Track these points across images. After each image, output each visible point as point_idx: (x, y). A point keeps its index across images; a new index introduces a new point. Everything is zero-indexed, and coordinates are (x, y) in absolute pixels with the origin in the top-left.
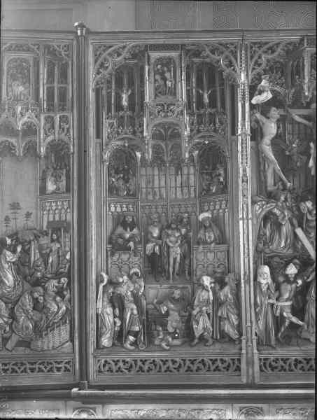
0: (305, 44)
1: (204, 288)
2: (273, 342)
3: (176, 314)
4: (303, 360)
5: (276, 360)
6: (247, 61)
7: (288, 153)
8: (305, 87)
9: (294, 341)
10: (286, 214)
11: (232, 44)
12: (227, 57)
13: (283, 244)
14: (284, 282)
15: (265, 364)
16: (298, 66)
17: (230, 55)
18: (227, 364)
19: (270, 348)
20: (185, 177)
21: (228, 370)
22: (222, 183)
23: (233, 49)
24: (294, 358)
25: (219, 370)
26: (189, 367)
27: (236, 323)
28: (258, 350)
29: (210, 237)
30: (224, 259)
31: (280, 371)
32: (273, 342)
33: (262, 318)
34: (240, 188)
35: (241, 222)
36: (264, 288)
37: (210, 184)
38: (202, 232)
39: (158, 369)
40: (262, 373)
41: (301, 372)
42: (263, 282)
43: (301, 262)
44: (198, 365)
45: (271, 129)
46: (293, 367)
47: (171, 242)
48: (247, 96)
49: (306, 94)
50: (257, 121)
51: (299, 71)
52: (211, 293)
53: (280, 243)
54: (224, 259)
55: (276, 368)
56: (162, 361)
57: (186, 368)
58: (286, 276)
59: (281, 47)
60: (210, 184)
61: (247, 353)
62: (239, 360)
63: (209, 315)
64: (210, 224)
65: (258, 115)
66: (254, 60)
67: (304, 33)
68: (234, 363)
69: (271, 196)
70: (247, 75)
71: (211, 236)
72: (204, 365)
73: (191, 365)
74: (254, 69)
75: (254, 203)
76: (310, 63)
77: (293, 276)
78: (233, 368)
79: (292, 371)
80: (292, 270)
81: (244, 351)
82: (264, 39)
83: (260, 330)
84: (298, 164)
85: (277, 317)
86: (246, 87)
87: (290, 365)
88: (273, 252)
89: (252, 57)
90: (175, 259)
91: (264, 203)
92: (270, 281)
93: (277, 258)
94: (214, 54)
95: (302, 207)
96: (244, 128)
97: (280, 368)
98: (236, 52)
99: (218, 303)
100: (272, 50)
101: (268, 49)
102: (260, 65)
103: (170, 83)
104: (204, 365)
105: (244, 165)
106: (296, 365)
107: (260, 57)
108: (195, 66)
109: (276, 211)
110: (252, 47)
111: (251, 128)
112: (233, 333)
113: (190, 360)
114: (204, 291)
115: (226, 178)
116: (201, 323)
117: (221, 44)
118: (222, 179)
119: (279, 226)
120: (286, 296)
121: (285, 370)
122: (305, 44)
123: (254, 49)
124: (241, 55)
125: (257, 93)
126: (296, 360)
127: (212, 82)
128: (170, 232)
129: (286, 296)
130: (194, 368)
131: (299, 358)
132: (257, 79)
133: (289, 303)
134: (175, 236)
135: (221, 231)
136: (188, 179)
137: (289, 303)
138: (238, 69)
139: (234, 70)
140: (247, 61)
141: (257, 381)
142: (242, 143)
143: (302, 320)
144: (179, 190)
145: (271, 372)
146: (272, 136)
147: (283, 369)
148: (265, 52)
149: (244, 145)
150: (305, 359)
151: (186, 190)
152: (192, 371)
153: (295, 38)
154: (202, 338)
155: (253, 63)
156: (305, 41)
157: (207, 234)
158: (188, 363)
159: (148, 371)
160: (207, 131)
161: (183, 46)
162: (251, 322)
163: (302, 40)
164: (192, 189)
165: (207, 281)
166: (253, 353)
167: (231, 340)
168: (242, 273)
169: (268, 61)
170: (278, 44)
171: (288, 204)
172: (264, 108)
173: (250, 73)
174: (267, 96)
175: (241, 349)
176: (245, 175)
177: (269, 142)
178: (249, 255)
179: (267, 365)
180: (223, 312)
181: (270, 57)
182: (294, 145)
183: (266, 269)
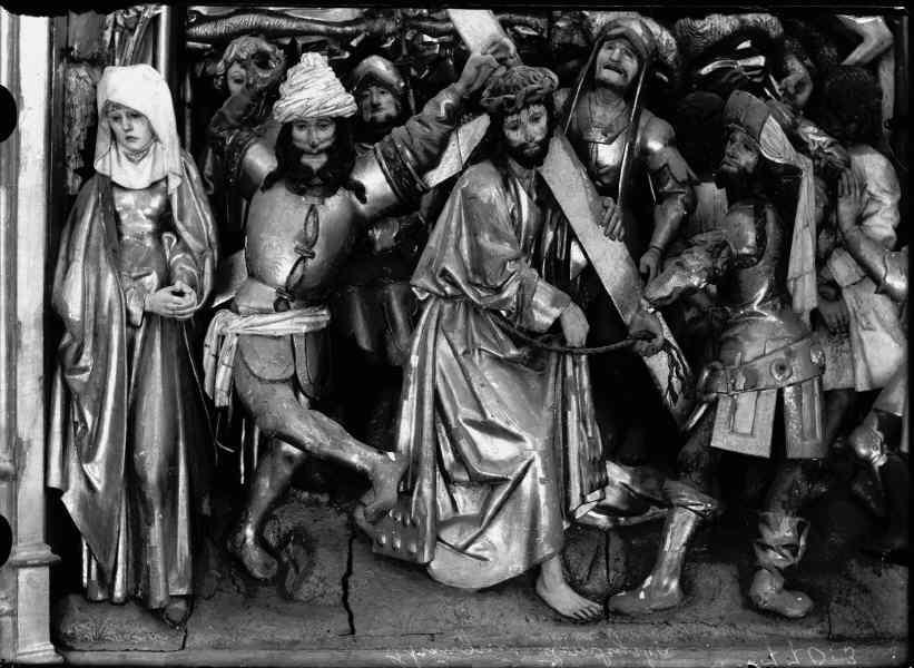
9: (328, 565)
14: (272, 180)
32: (168, 584)
36: (138, 217)
42: (129, 173)
77: (325, 136)
92: (169, 158)
120: (283, 264)
133: (294, 323)
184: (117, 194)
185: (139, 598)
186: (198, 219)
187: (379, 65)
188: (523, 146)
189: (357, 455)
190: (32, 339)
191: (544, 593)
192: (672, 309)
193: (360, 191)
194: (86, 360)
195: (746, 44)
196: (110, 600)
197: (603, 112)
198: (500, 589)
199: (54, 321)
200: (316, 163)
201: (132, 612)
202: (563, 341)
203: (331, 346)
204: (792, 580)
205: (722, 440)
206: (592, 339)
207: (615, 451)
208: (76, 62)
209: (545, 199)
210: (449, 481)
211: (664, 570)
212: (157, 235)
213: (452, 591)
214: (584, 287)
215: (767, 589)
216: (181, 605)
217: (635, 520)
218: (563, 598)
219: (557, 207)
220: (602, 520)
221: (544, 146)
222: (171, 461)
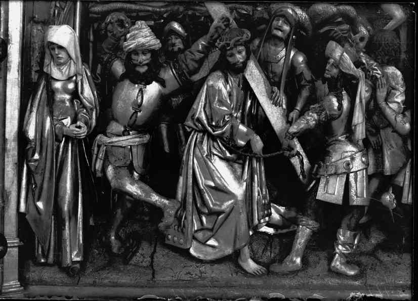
9: (145, 249)
14: (124, 77)
133: (131, 140)
143: (169, 193)
184: (53, 82)
185: (58, 262)
188: (235, 64)
191: (241, 263)
192: (303, 136)
194: (36, 156)
195: (340, 19)
200: (143, 70)
201: (56, 268)
202: (252, 151)
203: (152, 151)
204: (349, 261)
205: (321, 195)
206: (265, 150)
208: (37, 23)
209: (246, 88)
210: (200, 213)
211: (293, 253)
212: (71, 101)
213: (193, 258)
216: (78, 266)
217: (285, 231)
218: (251, 265)
219: (251, 90)
220: (271, 231)
221: (245, 64)
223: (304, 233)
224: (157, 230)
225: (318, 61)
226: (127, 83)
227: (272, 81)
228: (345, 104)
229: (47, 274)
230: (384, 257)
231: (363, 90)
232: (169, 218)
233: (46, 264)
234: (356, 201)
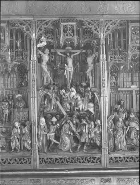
0: (61, 21)
1: (16, 127)
2: (45, 151)
3: (4, 139)
4: (80, 158)
5: (47, 159)
6: (35, 29)
7: (55, 69)
8: (61, 39)
9: (55, 150)
10: (54, 95)
11: (29, 21)
12: (27, 26)
13: (52, 108)
14: (51, 125)
15: (42, 161)
16: (59, 31)
17: (28, 26)
18: (25, 161)
19: (44, 154)
20: (12, 79)
21: (26, 163)
22: (27, 81)
23: (29, 23)
24: (55, 158)
25: (22, 163)
26: (9, 162)
27: (30, 142)
28: (39, 154)
29: (21, 105)
30: (27, 115)
31: (49, 163)
32: (45, 151)
33: (41, 141)
34: (32, 83)
35: (32, 99)
36: (43, 127)
37: (22, 82)
38: (17, 103)
39: (17, 162)
40: (40, 164)
41: (58, 164)
42: (42, 125)
43: (60, 116)
44: (13, 161)
45: (46, 58)
46: (55, 162)
47: (4, 107)
48: (35, 44)
49: (61, 43)
50: (40, 55)
51: (59, 33)
52: (19, 129)
53: (51, 108)
54: (27, 115)
55: (47, 162)
56: (19, 159)
57: (8, 163)
58: (52, 122)
59: (50, 22)
60: (22, 82)
61: (34, 156)
62: (31, 159)
63: (18, 139)
64: (21, 100)
65: (40, 52)
66: (39, 27)
67: (60, 16)
68: (29, 160)
69: (47, 88)
70: (35, 35)
71: (22, 104)
72: (16, 161)
73: (10, 161)
74: (38, 32)
75: (38, 90)
76: (63, 30)
77: (55, 122)
78: (28, 162)
79: (54, 163)
80: (54, 119)
81: (33, 155)
82: (43, 19)
83: (40, 146)
84: (60, 73)
85: (48, 140)
86: (35, 40)
87: (53, 161)
88: (48, 112)
89: (38, 27)
90: (6, 115)
91: (43, 90)
92: (45, 124)
93: (49, 114)
94: (21, 25)
95: (60, 93)
96: (34, 57)
97: (49, 162)
98: (31, 25)
99: (22, 134)
100: (47, 24)
101: (45, 23)
102: (41, 30)
103: (2, 37)
104: (16, 161)
105: (33, 74)
106: (56, 161)
107: (41, 27)
108: (15, 30)
109: (49, 94)
110: (38, 22)
111: (37, 57)
112: (28, 147)
113: (9, 159)
114: (16, 129)
115: (28, 80)
116: (14, 142)
117: (25, 21)
118: (26, 80)
119: (50, 100)
121: (51, 163)
122: (61, 21)
123: (38, 23)
124: (33, 26)
125: (39, 42)
126: (56, 159)
127: (22, 37)
128: (3, 103)
129: (52, 131)
130: (11, 162)
131: (57, 158)
132: (40, 36)
134: (5, 104)
135: (26, 103)
136: (13, 79)
137: (53, 134)
138: (31, 31)
139: (30, 32)
140: (35, 29)
141: (38, 167)
142: (32, 64)
143: (59, 141)
144: (9, 84)
145: (45, 164)
146: (47, 61)
147: (50, 162)
148: (43, 25)
149: (33, 65)
150: (60, 158)
151: (12, 85)
152: (10, 164)
153: (57, 19)
154: (15, 149)
155: (38, 29)
156: (61, 20)
157: (20, 104)
158: (9, 160)
159: (13, 164)
160: (19, 59)
161: (8, 22)
162: (36, 142)
163: (60, 19)
164: (15, 84)
165: (17, 124)
166: (36, 156)
167: (28, 150)
168: (32, 121)
169: (45, 28)
170: (49, 21)
171: (55, 91)
172: (42, 49)
173: (37, 33)
174: (44, 44)
175: (31, 154)
176: (34, 78)
177: (45, 64)
178: (35, 113)
179: (43, 161)
180: (24, 138)
181: (46, 26)
182: (58, 65)
183: (43, 119)
186: (46, 127)
187: (58, 116)
189: (58, 142)
190: (37, 136)
192: (79, 133)
193: (57, 125)
196: (41, 152)
197: (74, 119)
198: (67, 151)
199: (38, 134)
204: (86, 150)
205: (81, 141)
207: (75, 142)
214: (73, 132)
215: (84, 151)
218: (71, 152)
221: (70, 122)
222: (45, 143)
223: (79, 147)
224: (57, 148)
225: (81, 121)
226: (52, 126)
227: (74, 124)
228: (85, 127)
229: (42, 153)
230: (91, 150)
231: (87, 126)
232: (60, 145)
233: (41, 152)
234: (87, 142)
